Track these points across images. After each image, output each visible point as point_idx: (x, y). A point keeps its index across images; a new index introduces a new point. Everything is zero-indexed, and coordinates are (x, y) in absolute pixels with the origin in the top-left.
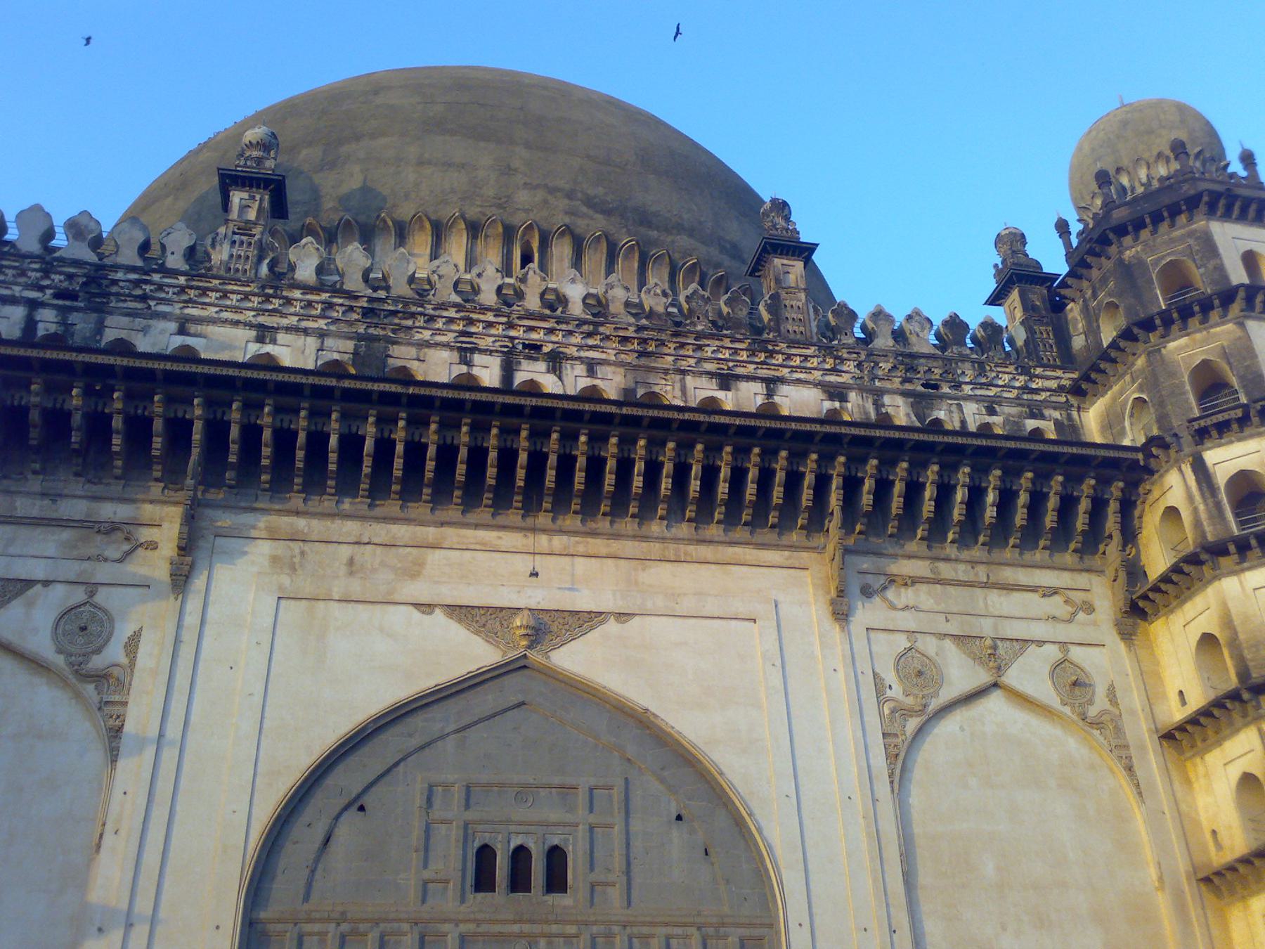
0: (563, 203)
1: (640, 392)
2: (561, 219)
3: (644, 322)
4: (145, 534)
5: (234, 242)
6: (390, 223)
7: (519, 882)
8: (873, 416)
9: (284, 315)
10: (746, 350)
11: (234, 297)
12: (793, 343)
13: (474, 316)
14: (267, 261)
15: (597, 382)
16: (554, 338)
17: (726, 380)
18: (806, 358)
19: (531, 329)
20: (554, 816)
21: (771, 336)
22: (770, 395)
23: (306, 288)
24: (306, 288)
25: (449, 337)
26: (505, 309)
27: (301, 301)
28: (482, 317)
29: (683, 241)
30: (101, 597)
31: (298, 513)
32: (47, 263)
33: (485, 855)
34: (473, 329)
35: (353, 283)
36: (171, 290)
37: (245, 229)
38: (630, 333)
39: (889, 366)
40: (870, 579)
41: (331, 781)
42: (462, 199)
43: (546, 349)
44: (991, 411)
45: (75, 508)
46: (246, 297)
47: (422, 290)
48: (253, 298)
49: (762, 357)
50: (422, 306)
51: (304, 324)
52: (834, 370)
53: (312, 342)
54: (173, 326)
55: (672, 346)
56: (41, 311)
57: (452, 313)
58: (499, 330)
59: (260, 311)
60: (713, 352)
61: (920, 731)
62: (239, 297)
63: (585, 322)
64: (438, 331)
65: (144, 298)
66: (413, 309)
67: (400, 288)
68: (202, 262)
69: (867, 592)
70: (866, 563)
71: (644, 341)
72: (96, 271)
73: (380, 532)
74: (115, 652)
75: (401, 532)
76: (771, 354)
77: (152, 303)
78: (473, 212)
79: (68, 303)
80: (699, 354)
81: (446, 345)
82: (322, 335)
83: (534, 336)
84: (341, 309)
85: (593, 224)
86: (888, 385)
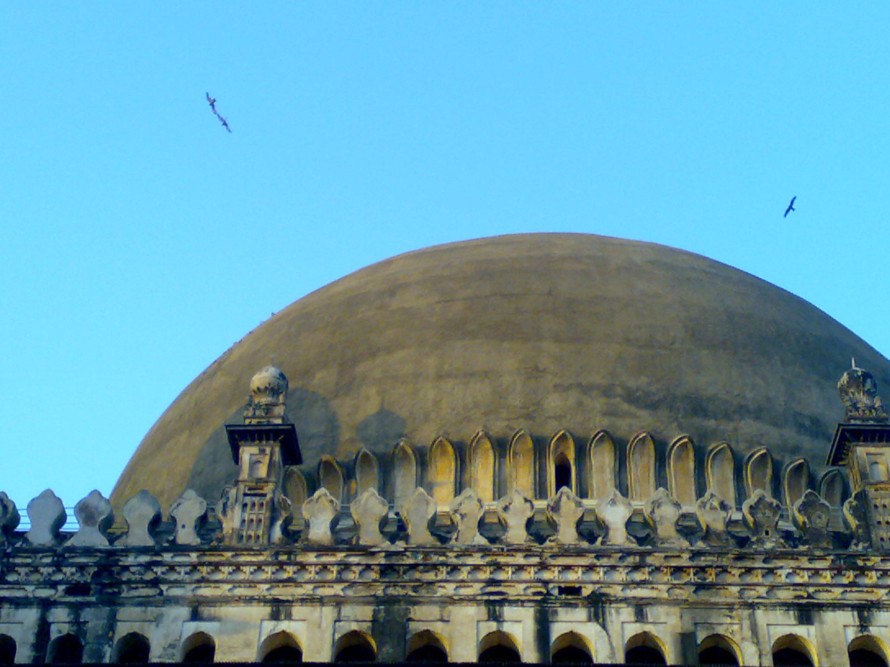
5: (245, 505)
6: (410, 451)
9: (298, 584)
10: (830, 569)
11: (247, 569)
13: (502, 560)
14: (279, 523)
16: (594, 577)
19: (568, 568)
21: (860, 547)
23: (322, 549)
24: (322, 549)
25: (475, 589)
26: (536, 547)
27: (316, 565)
28: (510, 560)
32: (58, 556)
34: (501, 576)
35: (370, 536)
36: (183, 570)
38: (684, 561)
43: (586, 592)
46: (259, 567)
47: (442, 531)
48: (266, 568)
49: (850, 576)
50: (444, 555)
51: (321, 592)
55: (736, 572)
56: (53, 610)
57: (476, 559)
60: (788, 575)
62: (252, 569)
63: (626, 553)
65: (155, 583)
66: (435, 559)
68: (213, 530)
71: (702, 569)
72: (107, 558)
76: (862, 571)
77: (164, 587)
79: (80, 599)
80: (770, 580)
81: (472, 600)
83: (571, 576)
84: (357, 569)
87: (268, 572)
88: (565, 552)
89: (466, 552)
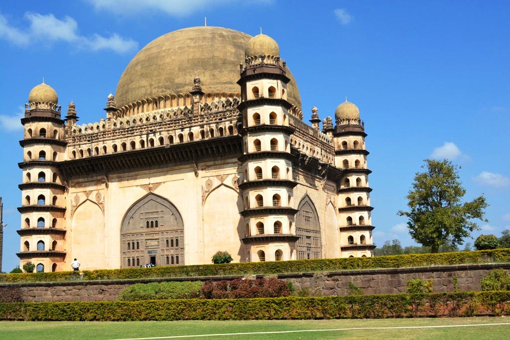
0: (160, 90)
1: (168, 135)
2: (161, 95)
3: (169, 119)
4: (103, 181)
7: (152, 226)
8: (209, 130)
12: (194, 117)
15: (162, 136)
17: (182, 129)
18: (197, 119)
20: (156, 216)
22: (190, 130)
25: (139, 133)
29: (186, 88)
30: (100, 191)
31: (120, 173)
33: (148, 222)
37: (109, 119)
39: (212, 117)
40: (203, 167)
41: (128, 214)
42: (145, 95)
44: (231, 123)
45: (95, 178)
46: (111, 134)
52: (203, 121)
53: (120, 140)
54: (102, 142)
57: (139, 128)
58: (146, 129)
59: (113, 136)
61: (209, 194)
64: (137, 132)
67: (132, 124)
69: (202, 170)
70: (203, 164)
71: (169, 124)
73: (130, 174)
74: (102, 200)
75: (133, 173)
76: (191, 120)
78: (146, 97)
82: (121, 138)
85: (168, 93)
86: (212, 122)
87: (112, 135)
88: (150, 125)
89: (137, 127)
